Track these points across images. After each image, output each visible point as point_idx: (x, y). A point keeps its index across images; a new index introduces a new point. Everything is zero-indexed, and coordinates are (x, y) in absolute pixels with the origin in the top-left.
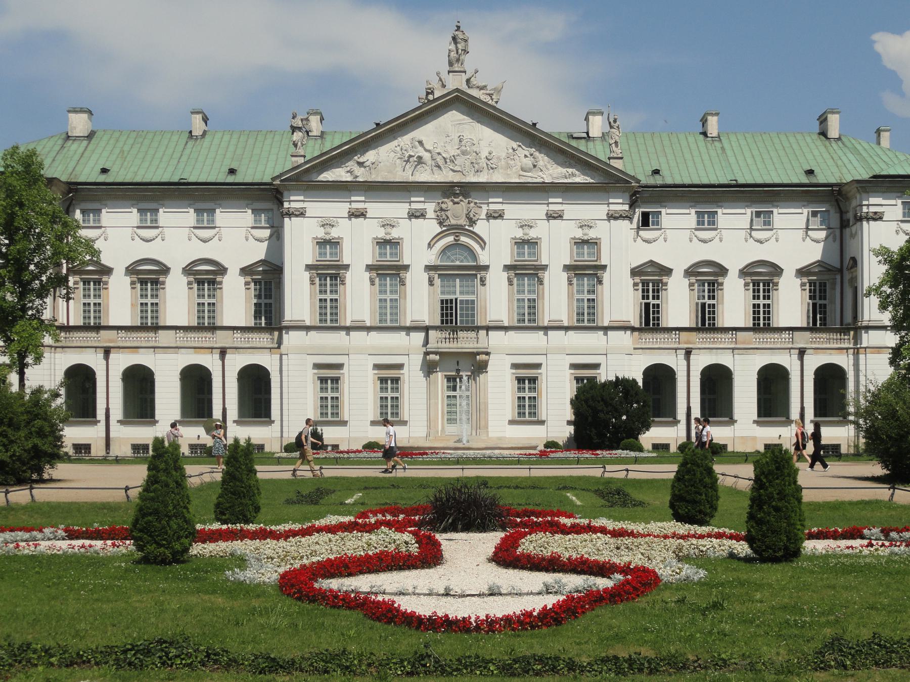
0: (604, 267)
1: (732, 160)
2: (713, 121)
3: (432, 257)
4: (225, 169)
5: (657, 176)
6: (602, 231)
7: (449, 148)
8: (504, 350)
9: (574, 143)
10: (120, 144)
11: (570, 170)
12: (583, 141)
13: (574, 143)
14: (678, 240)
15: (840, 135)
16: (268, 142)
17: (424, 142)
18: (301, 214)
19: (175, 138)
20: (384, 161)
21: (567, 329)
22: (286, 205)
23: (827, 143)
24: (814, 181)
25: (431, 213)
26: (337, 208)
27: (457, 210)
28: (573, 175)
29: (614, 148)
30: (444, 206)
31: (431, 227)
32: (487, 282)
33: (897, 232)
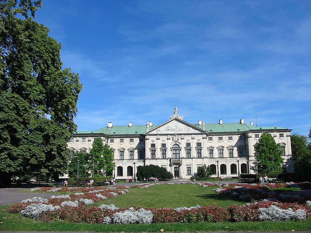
0: (202, 147)
1: (225, 128)
2: (221, 121)
3: (171, 146)
4: (135, 132)
5: (211, 131)
6: (201, 141)
7: (174, 127)
8: (185, 162)
9: (196, 126)
10: (117, 128)
11: (196, 130)
12: (198, 125)
13: (196, 126)
14: (215, 142)
15: (244, 123)
16: (143, 127)
17: (170, 126)
18: (148, 139)
19: (126, 127)
20: (162, 130)
21: (196, 158)
22: (146, 138)
23: (241, 125)
24: (239, 131)
25: (171, 139)
26: (154, 138)
27: (176, 138)
28: (196, 131)
29: (203, 127)
30: (173, 137)
31: (171, 141)
32: (181, 150)
33: (254, 140)
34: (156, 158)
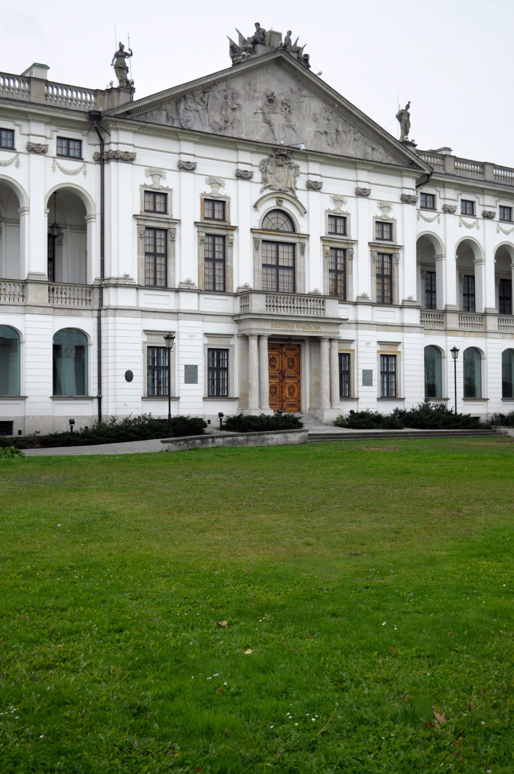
34: (170, 285)
